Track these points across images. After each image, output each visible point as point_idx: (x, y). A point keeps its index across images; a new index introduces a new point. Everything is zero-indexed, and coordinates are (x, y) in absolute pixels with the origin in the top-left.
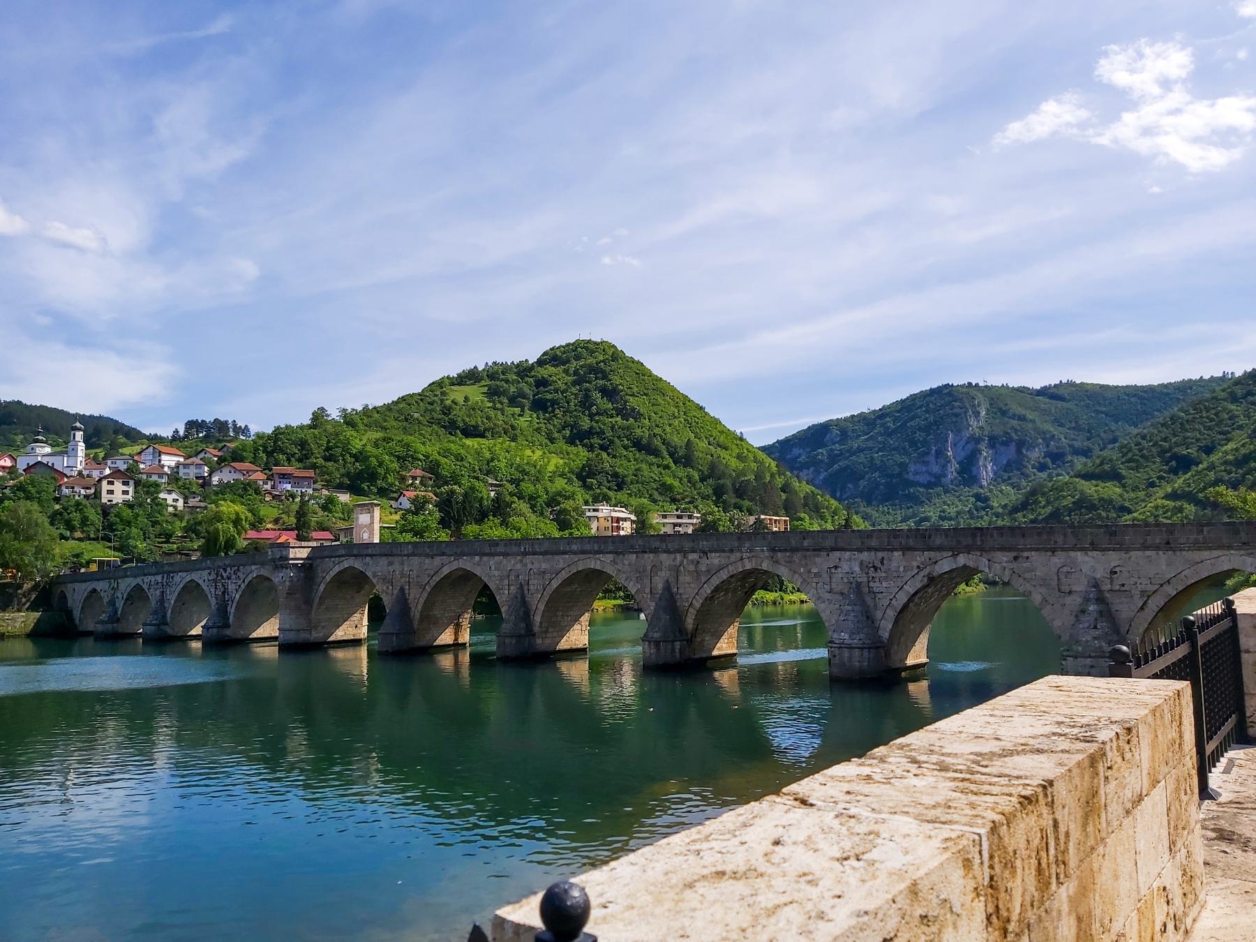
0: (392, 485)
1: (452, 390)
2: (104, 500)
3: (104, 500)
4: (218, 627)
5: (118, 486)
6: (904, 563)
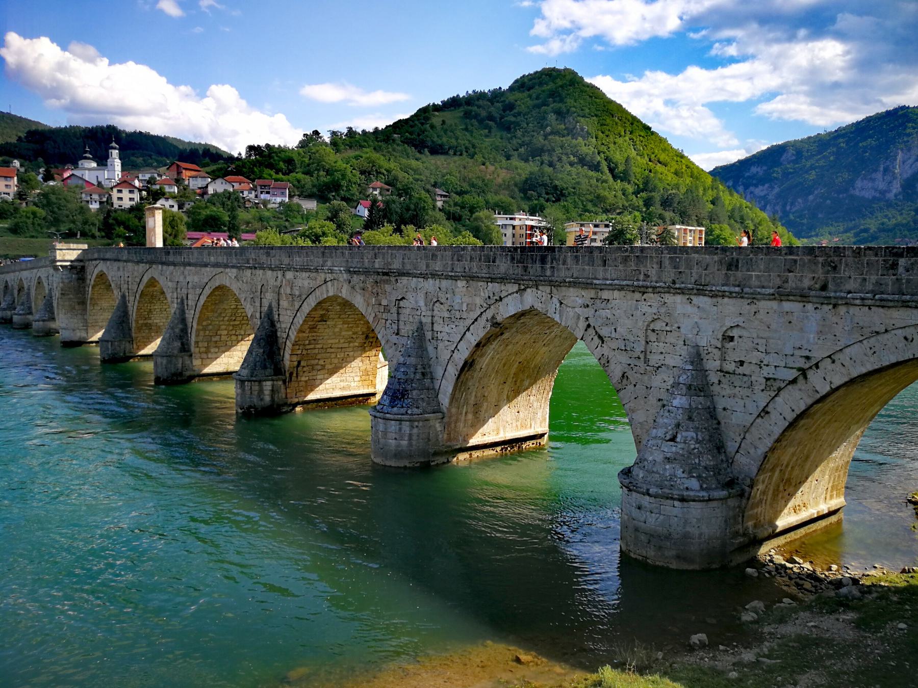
0: (353, 195)
1: (434, 116)
2: (116, 206)
3: (116, 206)
4: (44, 321)
5: (126, 194)
6: (467, 300)
